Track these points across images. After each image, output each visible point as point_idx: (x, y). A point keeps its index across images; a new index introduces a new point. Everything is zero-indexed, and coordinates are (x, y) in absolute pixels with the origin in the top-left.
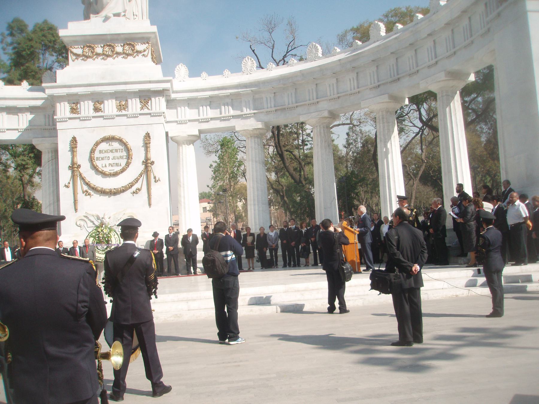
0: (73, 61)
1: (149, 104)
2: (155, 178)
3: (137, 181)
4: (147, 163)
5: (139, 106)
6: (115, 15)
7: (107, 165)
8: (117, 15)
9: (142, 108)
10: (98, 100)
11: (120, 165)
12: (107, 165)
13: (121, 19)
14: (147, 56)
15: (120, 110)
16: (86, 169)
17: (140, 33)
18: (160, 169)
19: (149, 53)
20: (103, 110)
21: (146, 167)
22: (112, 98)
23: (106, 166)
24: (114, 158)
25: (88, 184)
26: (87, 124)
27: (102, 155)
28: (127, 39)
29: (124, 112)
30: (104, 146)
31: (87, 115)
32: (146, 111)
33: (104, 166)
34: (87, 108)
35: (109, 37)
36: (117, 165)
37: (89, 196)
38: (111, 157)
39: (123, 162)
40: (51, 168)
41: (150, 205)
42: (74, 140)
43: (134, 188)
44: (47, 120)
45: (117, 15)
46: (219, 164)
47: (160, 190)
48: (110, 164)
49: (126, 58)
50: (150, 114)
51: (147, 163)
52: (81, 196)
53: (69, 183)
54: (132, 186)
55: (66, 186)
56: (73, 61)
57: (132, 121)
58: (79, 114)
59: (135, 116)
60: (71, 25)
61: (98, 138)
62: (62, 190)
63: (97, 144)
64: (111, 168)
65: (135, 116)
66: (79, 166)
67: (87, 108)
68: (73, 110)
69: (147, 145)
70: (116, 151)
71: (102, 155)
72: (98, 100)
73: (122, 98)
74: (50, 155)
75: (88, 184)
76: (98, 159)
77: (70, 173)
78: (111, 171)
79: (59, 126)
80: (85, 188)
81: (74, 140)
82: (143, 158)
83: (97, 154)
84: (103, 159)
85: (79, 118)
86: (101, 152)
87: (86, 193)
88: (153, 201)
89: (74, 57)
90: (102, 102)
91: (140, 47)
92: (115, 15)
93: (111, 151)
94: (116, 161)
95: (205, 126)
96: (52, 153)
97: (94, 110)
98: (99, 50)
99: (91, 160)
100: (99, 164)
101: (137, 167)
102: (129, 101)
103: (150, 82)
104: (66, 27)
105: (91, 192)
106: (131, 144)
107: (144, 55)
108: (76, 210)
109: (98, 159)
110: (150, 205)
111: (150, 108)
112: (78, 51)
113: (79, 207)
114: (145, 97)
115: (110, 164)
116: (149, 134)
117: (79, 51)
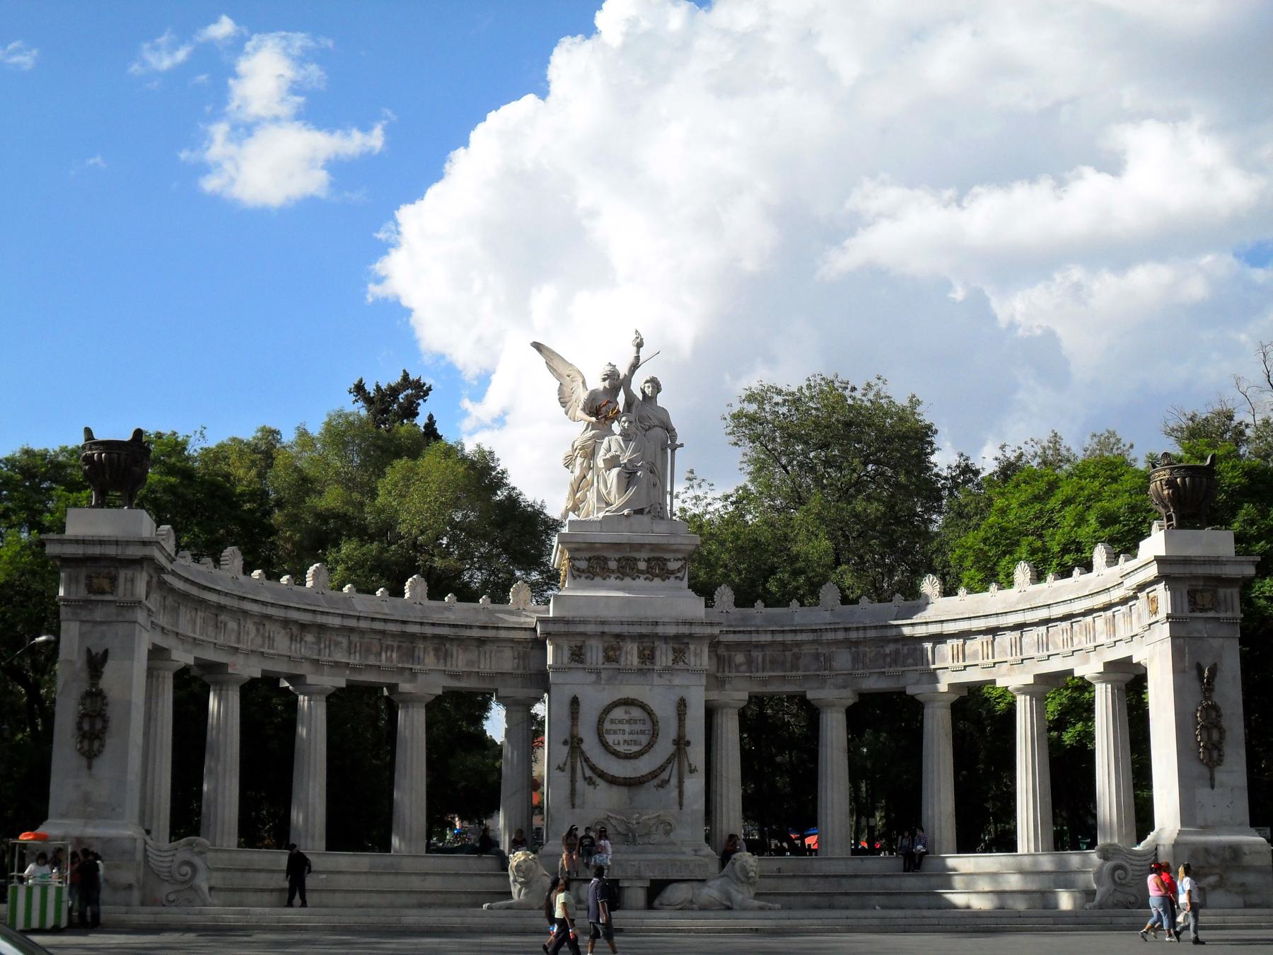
2: (690, 765)
4: (681, 743)
5: (671, 657)
9: (675, 661)
13: (645, 519)
21: (679, 749)
25: (593, 768)
27: (614, 727)
30: (618, 713)
37: (591, 787)
39: (644, 740)
41: (681, 805)
42: (575, 702)
51: (681, 743)
52: (581, 784)
58: (582, 662)
61: (609, 701)
64: (626, 747)
65: (668, 670)
66: (581, 740)
70: (635, 722)
71: (614, 727)
76: (608, 732)
77: (566, 749)
80: (588, 773)
83: (607, 725)
84: (615, 732)
86: (612, 722)
87: (590, 782)
88: (685, 802)
89: (575, 573)
93: (629, 722)
94: (635, 737)
95: (757, 689)
100: (610, 739)
101: (664, 747)
105: (598, 781)
106: (658, 712)
109: (608, 732)
113: (578, 802)
114: (680, 644)
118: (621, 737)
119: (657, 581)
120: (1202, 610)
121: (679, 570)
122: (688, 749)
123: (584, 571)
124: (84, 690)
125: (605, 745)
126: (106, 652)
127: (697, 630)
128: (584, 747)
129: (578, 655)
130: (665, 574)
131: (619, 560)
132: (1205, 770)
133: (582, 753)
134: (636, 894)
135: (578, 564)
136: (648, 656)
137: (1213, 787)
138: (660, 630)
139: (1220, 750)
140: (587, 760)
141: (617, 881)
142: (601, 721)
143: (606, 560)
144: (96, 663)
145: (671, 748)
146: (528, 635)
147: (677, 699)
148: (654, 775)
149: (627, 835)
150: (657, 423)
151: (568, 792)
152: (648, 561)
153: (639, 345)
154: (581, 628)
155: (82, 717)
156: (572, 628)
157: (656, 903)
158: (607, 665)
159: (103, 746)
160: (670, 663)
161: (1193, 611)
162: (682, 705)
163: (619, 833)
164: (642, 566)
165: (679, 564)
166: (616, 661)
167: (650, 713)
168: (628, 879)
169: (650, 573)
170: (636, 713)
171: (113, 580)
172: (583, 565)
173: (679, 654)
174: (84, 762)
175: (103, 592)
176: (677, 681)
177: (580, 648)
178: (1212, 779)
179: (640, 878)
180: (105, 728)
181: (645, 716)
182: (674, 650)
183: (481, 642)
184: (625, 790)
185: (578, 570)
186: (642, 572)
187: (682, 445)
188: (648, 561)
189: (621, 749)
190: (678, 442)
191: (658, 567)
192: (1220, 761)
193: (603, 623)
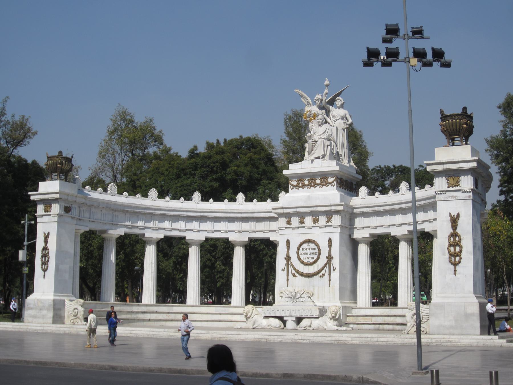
4: (330, 258)
8: (317, 158)
9: (327, 222)
10: (302, 216)
14: (334, 186)
15: (314, 223)
16: (294, 260)
19: (335, 183)
22: (310, 216)
25: (295, 269)
26: (296, 231)
27: (303, 252)
28: (322, 175)
30: (305, 246)
32: (330, 224)
34: (295, 221)
35: (311, 174)
39: (315, 257)
41: (330, 285)
42: (288, 242)
43: (320, 274)
45: (317, 158)
50: (332, 226)
51: (330, 258)
56: (292, 189)
57: (322, 230)
60: (291, 166)
61: (302, 241)
63: (301, 244)
64: (308, 260)
67: (295, 221)
68: (289, 223)
69: (330, 246)
70: (312, 249)
71: (303, 252)
72: (302, 216)
73: (315, 216)
75: (295, 269)
76: (301, 254)
80: (293, 272)
81: (288, 242)
82: (327, 255)
83: (301, 251)
86: (303, 249)
87: (294, 275)
89: (292, 187)
90: (304, 218)
91: (330, 180)
94: (311, 256)
99: (298, 253)
100: (302, 257)
102: (320, 217)
103: (331, 206)
104: (287, 168)
108: (288, 285)
109: (301, 254)
110: (330, 285)
112: (295, 183)
117: (295, 183)
119: (324, 187)
120: (453, 187)
121: (333, 182)
124: (42, 248)
125: (299, 259)
126: (49, 233)
127: (333, 208)
128: (292, 260)
130: (327, 184)
132: (452, 267)
133: (291, 263)
136: (316, 221)
137: (455, 274)
138: (319, 209)
139: (460, 256)
140: (293, 266)
142: (298, 249)
144: (47, 237)
145: (326, 260)
155: (42, 257)
158: (300, 225)
159: (48, 267)
161: (448, 187)
162: (330, 241)
165: (332, 179)
167: (317, 244)
169: (321, 185)
170: (312, 245)
171: (51, 208)
174: (43, 272)
175: (48, 211)
176: (328, 229)
178: (455, 271)
179: (291, 316)
180: (48, 261)
181: (316, 247)
184: (306, 279)
185: (292, 185)
186: (318, 184)
189: (306, 261)
191: (325, 183)
192: (460, 262)
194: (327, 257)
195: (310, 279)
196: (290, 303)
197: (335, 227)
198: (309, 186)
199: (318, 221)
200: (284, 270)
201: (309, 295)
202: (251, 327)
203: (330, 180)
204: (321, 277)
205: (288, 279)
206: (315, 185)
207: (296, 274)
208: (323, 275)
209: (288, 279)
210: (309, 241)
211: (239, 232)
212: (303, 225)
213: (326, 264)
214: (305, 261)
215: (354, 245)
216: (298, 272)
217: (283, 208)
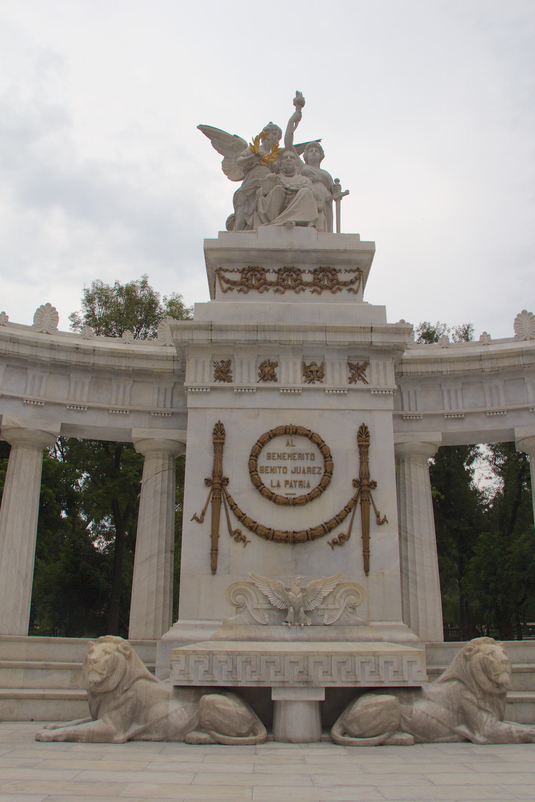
0: (225, 292)
1: (367, 372)
3: (342, 520)
5: (346, 373)
6: (298, 224)
7: (282, 484)
9: (352, 380)
11: (308, 486)
12: (282, 484)
17: (345, 251)
18: (385, 499)
20: (277, 377)
21: (361, 492)
23: (278, 485)
24: (295, 471)
25: (241, 518)
26: (246, 401)
27: (272, 463)
29: (317, 384)
30: (278, 446)
31: (245, 384)
32: (359, 385)
33: (275, 484)
36: (301, 484)
37: (241, 544)
38: (290, 468)
39: (315, 481)
40: (159, 486)
41: (367, 570)
42: (219, 432)
43: (334, 535)
44: (162, 398)
46: (495, 497)
47: (385, 540)
48: (287, 482)
49: (320, 293)
50: (369, 391)
51: (364, 486)
52: (225, 541)
53: (203, 514)
54: (330, 530)
55: (195, 518)
57: (334, 402)
59: (340, 393)
61: (267, 429)
62: (188, 526)
66: (225, 482)
70: (301, 456)
71: (272, 463)
74: (160, 462)
76: (265, 470)
77: (206, 492)
78: (289, 497)
79: (192, 402)
80: (236, 525)
81: (219, 432)
83: (262, 461)
84: (273, 470)
85: (232, 389)
86: (270, 456)
87: (238, 536)
89: (225, 286)
92: (298, 224)
93: (292, 456)
94: (299, 477)
96: (164, 459)
97: (259, 375)
98: (271, 277)
100: (266, 479)
101: (340, 492)
107: (350, 290)
108: (214, 570)
109: (265, 470)
110: (367, 570)
111: (367, 379)
115: (287, 482)
116: (366, 428)
118: (280, 477)
119: (326, 294)
121: (352, 282)
122: (373, 492)
123: (234, 283)
125: (259, 486)
128: (230, 489)
129: (223, 373)
131: (278, 272)
133: (228, 497)
134: (298, 714)
135: (228, 276)
138: (331, 338)
140: (233, 507)
141: (268, 691)
142: (254, 455)
143: (264, 271)
145: (351, 492)
146: (169, 366)
147: (357, 429)
148: (327, 528)
149: (286, 611)
150: (320, 178)
151: (207, 551)
152: (315, 272)
153: (299, 102)
154: (231, 336)
156: (216, 336)
157: (336, 731)
158: (262, 384)
160: (345, 383)
162: (363, 434)
163: (274, 608)
164: (307, 278)
166: (273, 377)
168: (284, 686)
169: (317, 286)
170: (303, 445)
172: (236, 277)
173: (357, 371)
177: (229, 362)
179: (308, 684)
182: (351, 366)
183: (114, 373)
185: (228, 281)
187: (347, 193)
188: (315, 272)
190: (343, 191)
193: (257, 329)
194: (357, 483)
195: (299, 547)
196: (281, 632)
197: (379, 393)
198: (281, 286)
199: (323, 375)
200: (200, 521)
201: (352, 599)
202: (121, 737)
203: (343, 277)
204: (334, 543)
205: (214, 551)
206: (298, 286)
207: (245, 532)
208: (342, 540)
209: (214, 551)
210: (291, 432)
211: (36, 404)
212: (271, 384)
213: (354, 501)
214: (276, 491)
215: (400, 459)
216: (254, 528)
217: (210, 328)
